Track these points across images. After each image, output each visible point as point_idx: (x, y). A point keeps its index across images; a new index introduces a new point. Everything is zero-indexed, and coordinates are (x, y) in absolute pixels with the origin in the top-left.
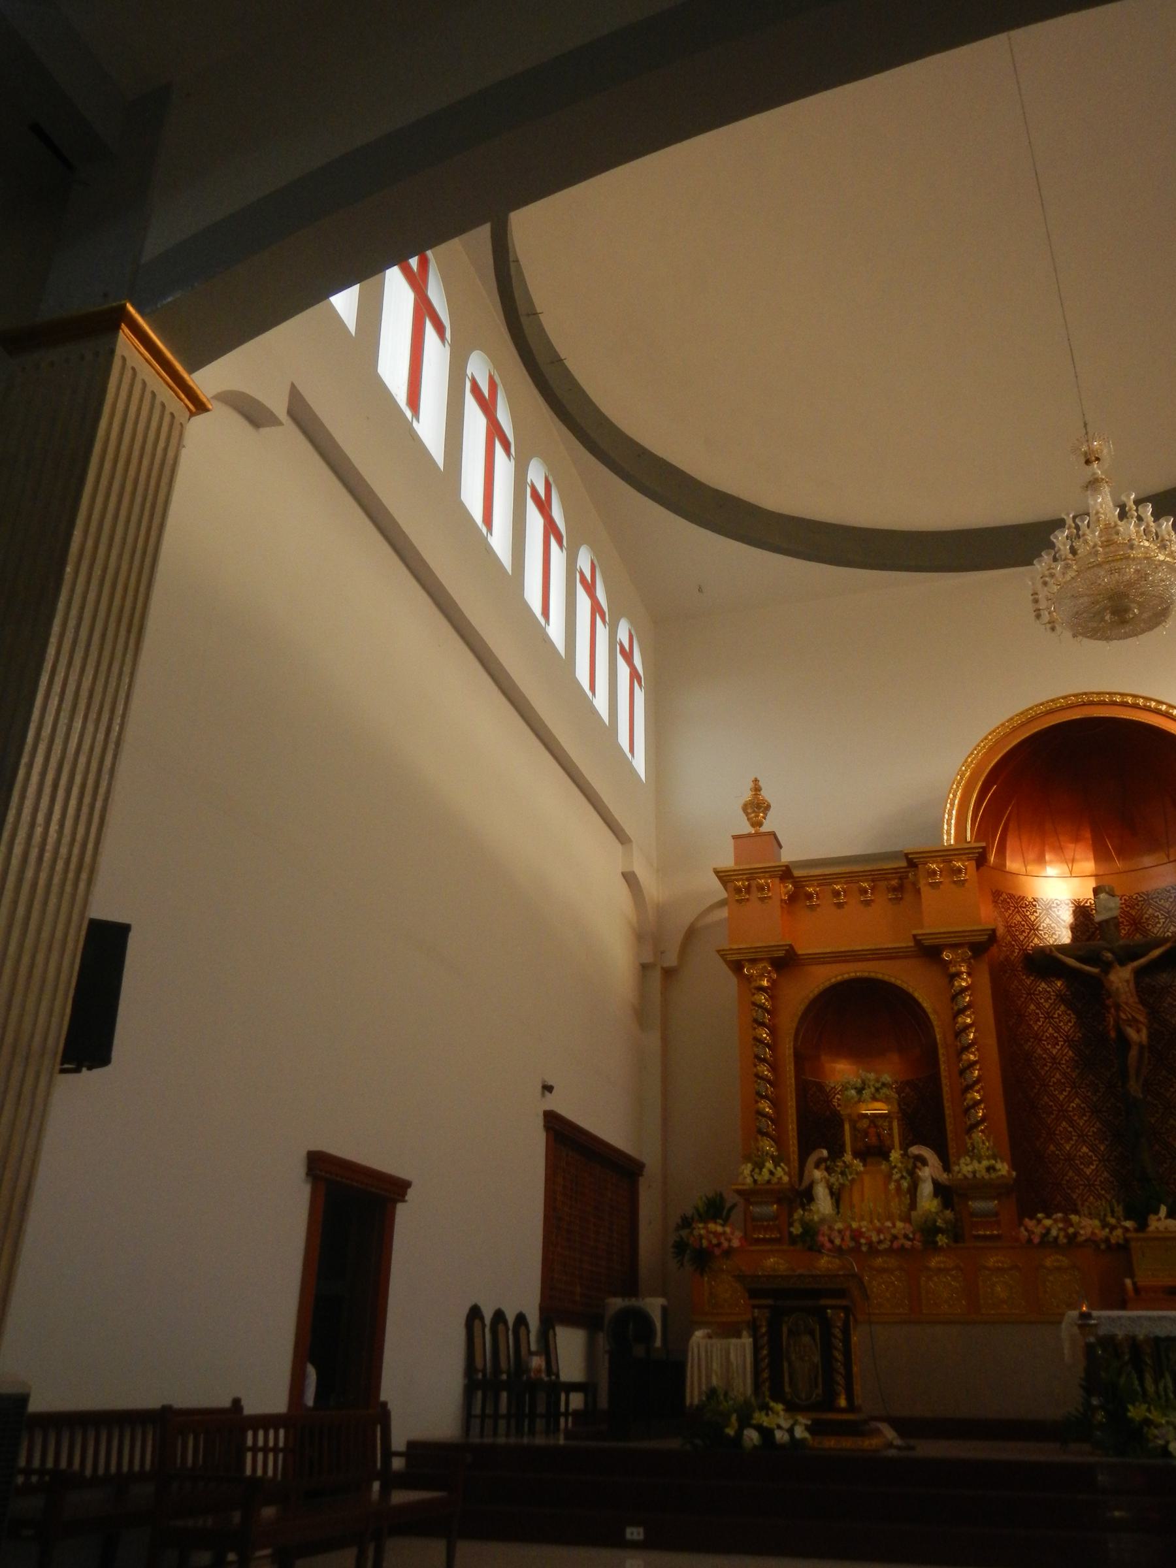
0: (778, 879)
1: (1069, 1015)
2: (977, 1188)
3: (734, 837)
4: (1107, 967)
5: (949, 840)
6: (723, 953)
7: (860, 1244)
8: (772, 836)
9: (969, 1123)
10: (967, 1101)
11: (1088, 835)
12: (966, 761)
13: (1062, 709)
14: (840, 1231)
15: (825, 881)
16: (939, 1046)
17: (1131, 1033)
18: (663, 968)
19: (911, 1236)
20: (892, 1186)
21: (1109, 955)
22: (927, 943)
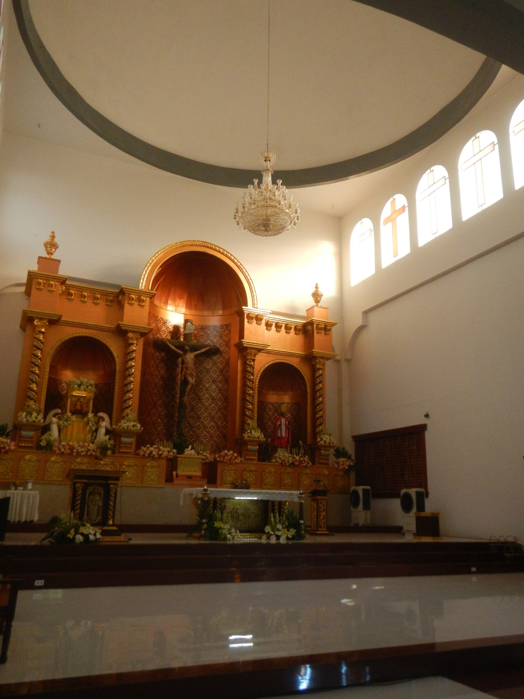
0: (60, 283)
1: (164, 367)
2: (128, 433)
3: (40, 258)
4: (185, 352)
5: (142, 287)
7: (72, 452)
9: (125, 406)
10: (126, 397)
11: (186, 297)
12: (155, 255)
13: (196, 245)
14: (64, 446)
15: (80, 289)
16: (117, 372)
17: (190, 379)
19: (95, 450)
20: (88, 428)
21: (188, 347)
22: (123, 328)
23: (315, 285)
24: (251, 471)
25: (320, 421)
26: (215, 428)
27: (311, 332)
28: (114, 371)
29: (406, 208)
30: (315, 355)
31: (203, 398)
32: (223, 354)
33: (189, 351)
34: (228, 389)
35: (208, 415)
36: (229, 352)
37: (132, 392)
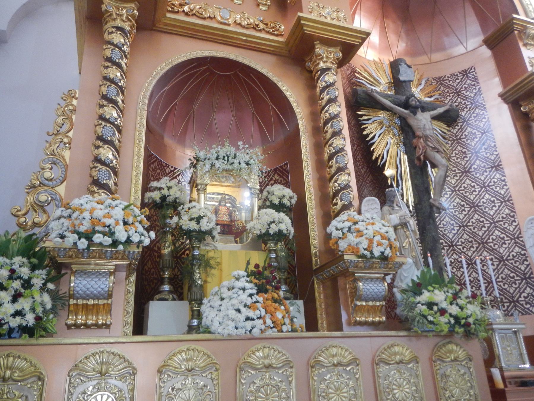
22: (307, 30)
32: (470, 122)
33: (419, 110)
34: (504, 180)
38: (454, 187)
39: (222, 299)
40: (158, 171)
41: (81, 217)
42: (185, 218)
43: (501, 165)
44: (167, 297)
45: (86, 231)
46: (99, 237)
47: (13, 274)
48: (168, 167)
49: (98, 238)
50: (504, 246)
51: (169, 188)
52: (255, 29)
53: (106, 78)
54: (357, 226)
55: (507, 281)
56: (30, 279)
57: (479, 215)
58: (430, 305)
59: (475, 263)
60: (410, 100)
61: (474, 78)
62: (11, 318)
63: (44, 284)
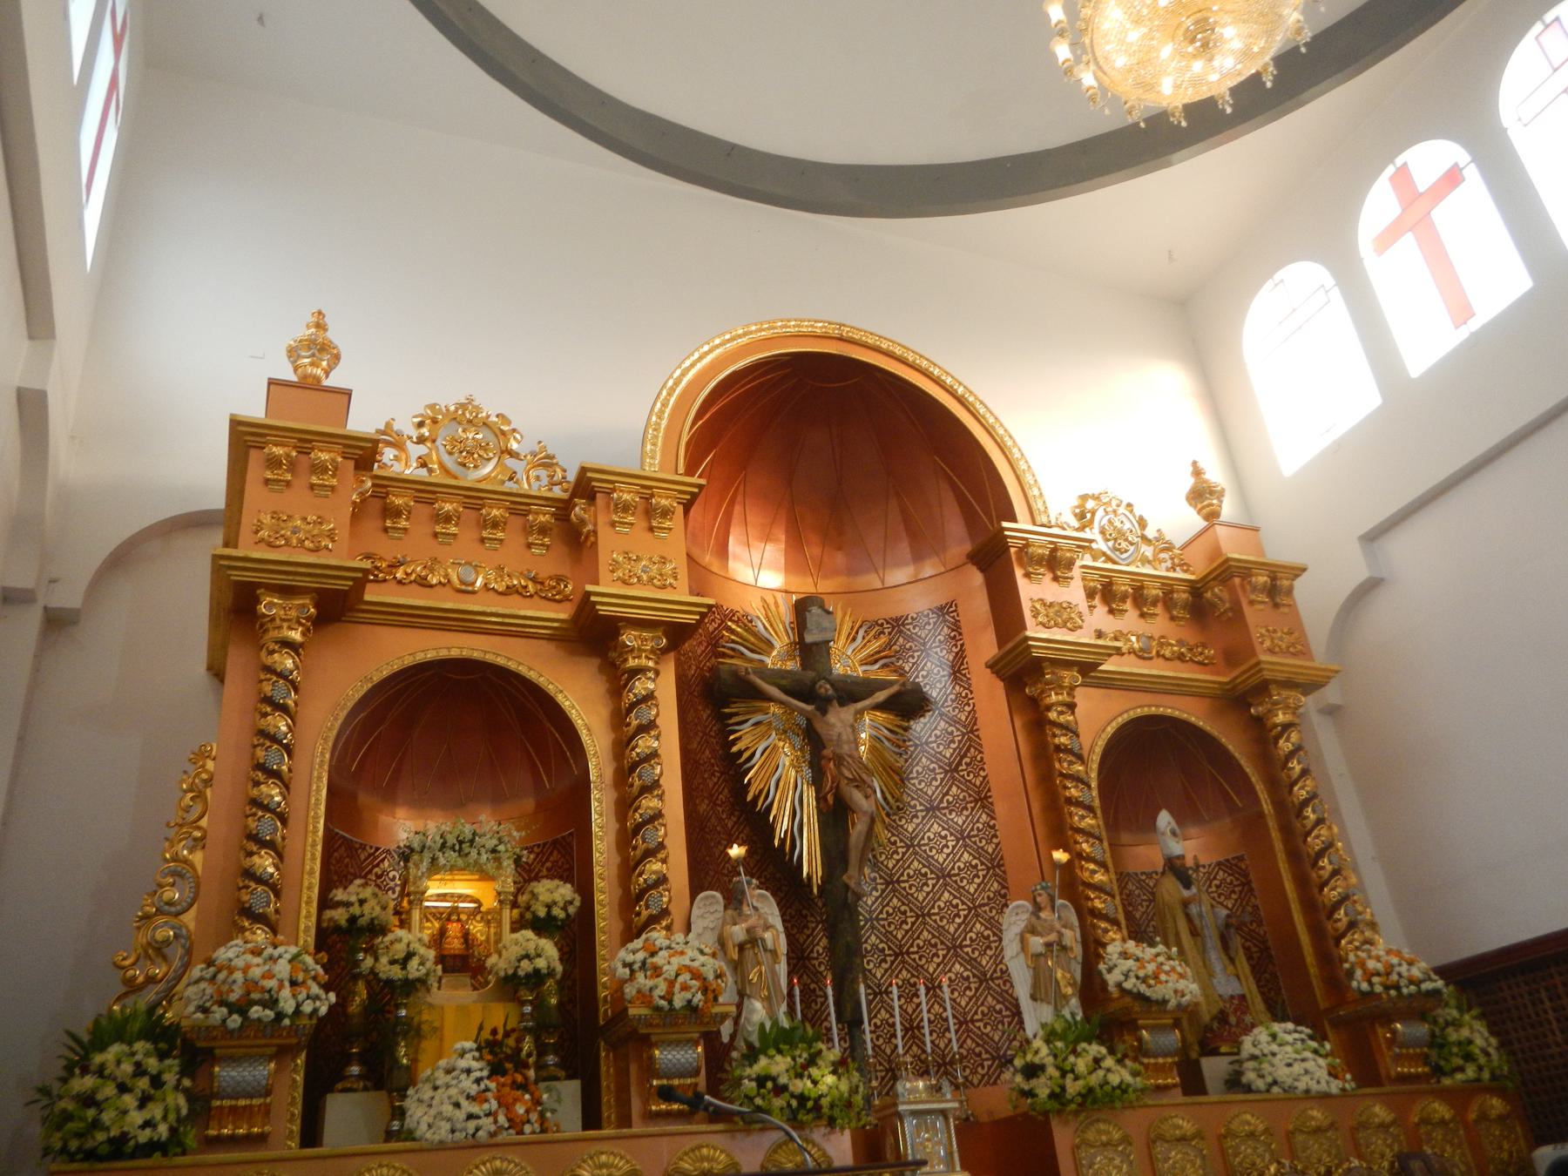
0: (351, 464)
3: (272, 383)
4: (823, 705)
6: (222, 562)
8: (347, 397)
9: (645, 914)
18: (46, 609)
21: (828, 686)
22: (604, 610)
23: (1190, 469)
24: (1183, 1139)
25: (1346, 914)
26: (973, 986)
27: (1227, 605)
28: (582, 789)
29: (1464, 172)
30: (1267, 675)
31: (902, 875)
33: (835, 703)
34: (993, 827)
35: (934, 936)
36: (970, 696)
37: (661, 855)
38: (912, 839)
39: (436, 1088)
40: (347, 860)
41: (230, 980)
42: (384, 960)
43: (990, 797)
44: (355, 1086)
45: (238, 1000)
46: (257, 1012)
47: (140, 1071)
48: (364, 849)
49: (256, 1012)
50: (988, 952)
51: (362, 902)
52: (521, 594)
53: (263, 733)
54: (655, 960)
55: (990, 1019)
56: (159, 1074)
57: (951, 893)
58: (761, 1081)
59: (940, 987)
60: (817, 686)
61: (955, 624)
62: (139, 1131)
63: (179, 1081)
